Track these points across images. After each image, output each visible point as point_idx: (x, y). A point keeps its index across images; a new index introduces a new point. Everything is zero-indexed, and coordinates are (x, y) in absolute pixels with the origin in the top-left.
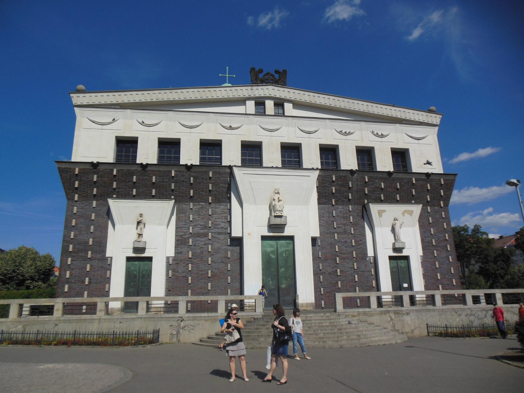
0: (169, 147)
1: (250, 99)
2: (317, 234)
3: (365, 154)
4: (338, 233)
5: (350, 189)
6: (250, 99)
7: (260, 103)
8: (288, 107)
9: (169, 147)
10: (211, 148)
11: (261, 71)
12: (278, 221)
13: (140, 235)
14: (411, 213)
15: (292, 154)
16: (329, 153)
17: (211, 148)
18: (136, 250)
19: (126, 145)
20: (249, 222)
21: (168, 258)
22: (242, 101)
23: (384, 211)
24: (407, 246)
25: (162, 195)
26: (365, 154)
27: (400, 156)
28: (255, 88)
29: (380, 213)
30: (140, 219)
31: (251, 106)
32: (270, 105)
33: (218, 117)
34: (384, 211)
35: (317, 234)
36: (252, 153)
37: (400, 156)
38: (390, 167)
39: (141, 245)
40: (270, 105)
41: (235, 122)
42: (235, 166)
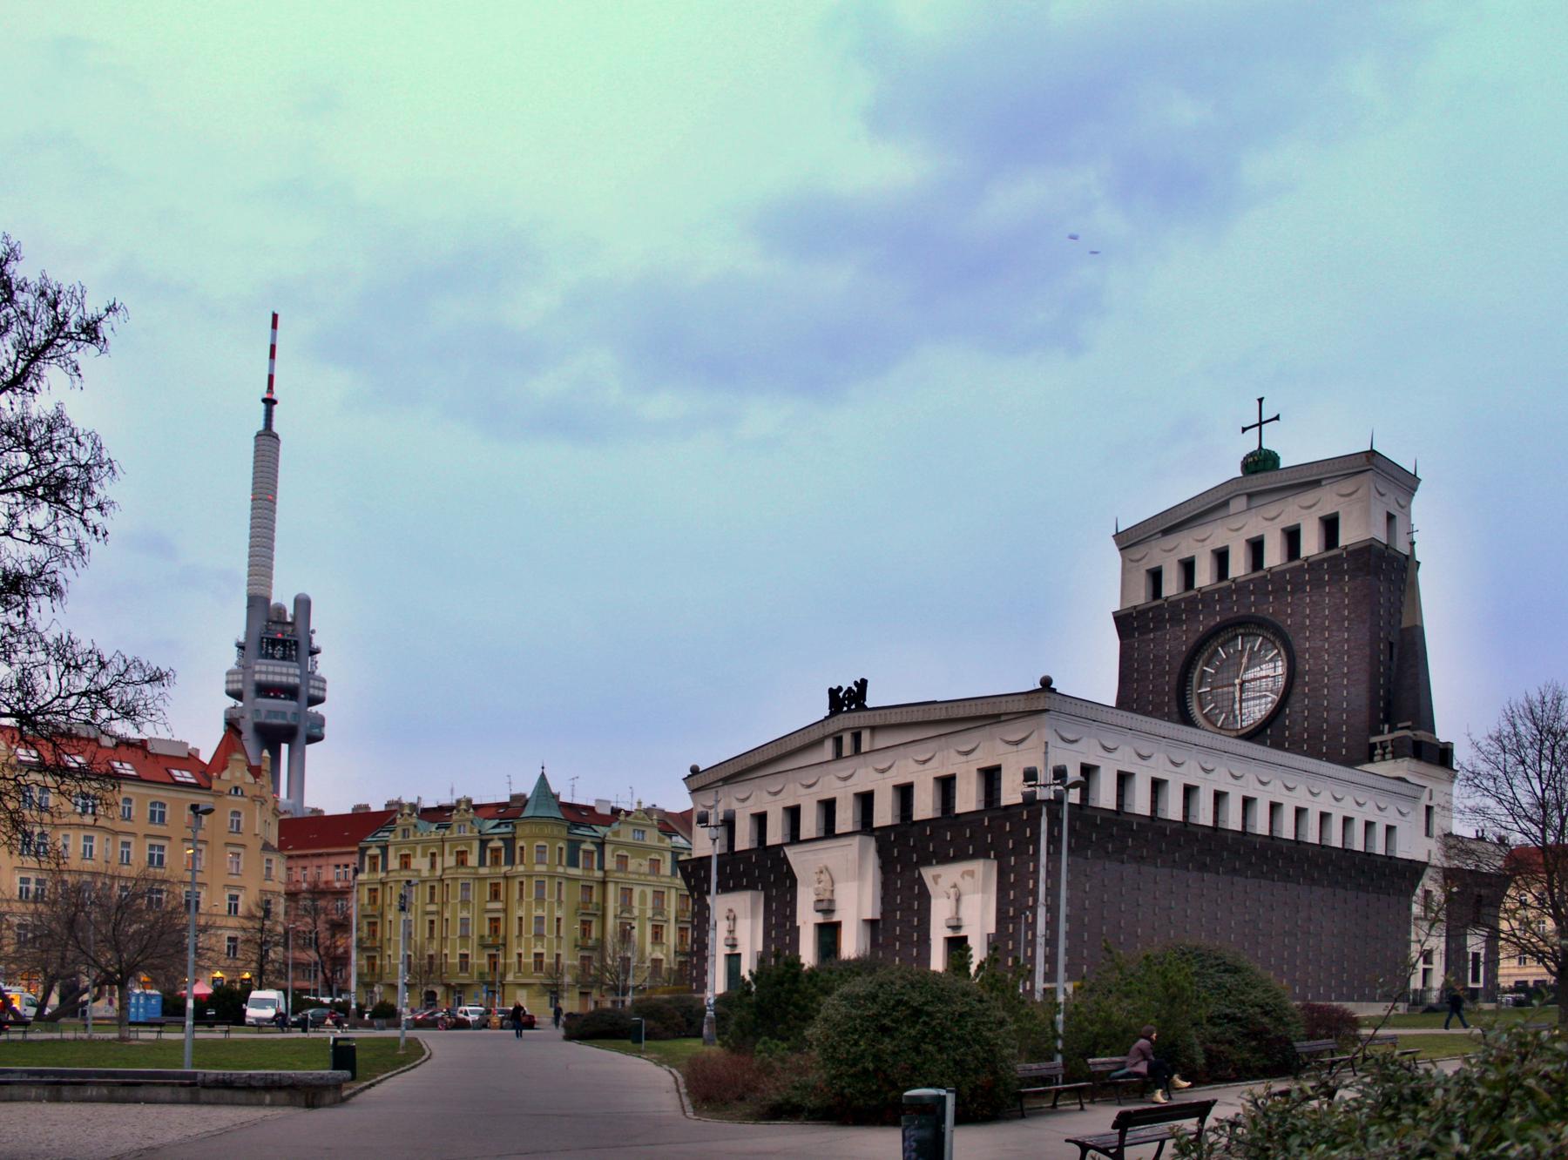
1: (826, 737)
4: (902, 911)
5: (907, 849)
6: (826, 737)
7: (838, 741)
8: (866, 736)
11: (840, 689)
14: (971, 874)
22: (819, 743)
24: (965, 922)
29: (936, 878)
31: (828, 750)
32: (847, 739)
33: (798, 774)
40: (847, 739)
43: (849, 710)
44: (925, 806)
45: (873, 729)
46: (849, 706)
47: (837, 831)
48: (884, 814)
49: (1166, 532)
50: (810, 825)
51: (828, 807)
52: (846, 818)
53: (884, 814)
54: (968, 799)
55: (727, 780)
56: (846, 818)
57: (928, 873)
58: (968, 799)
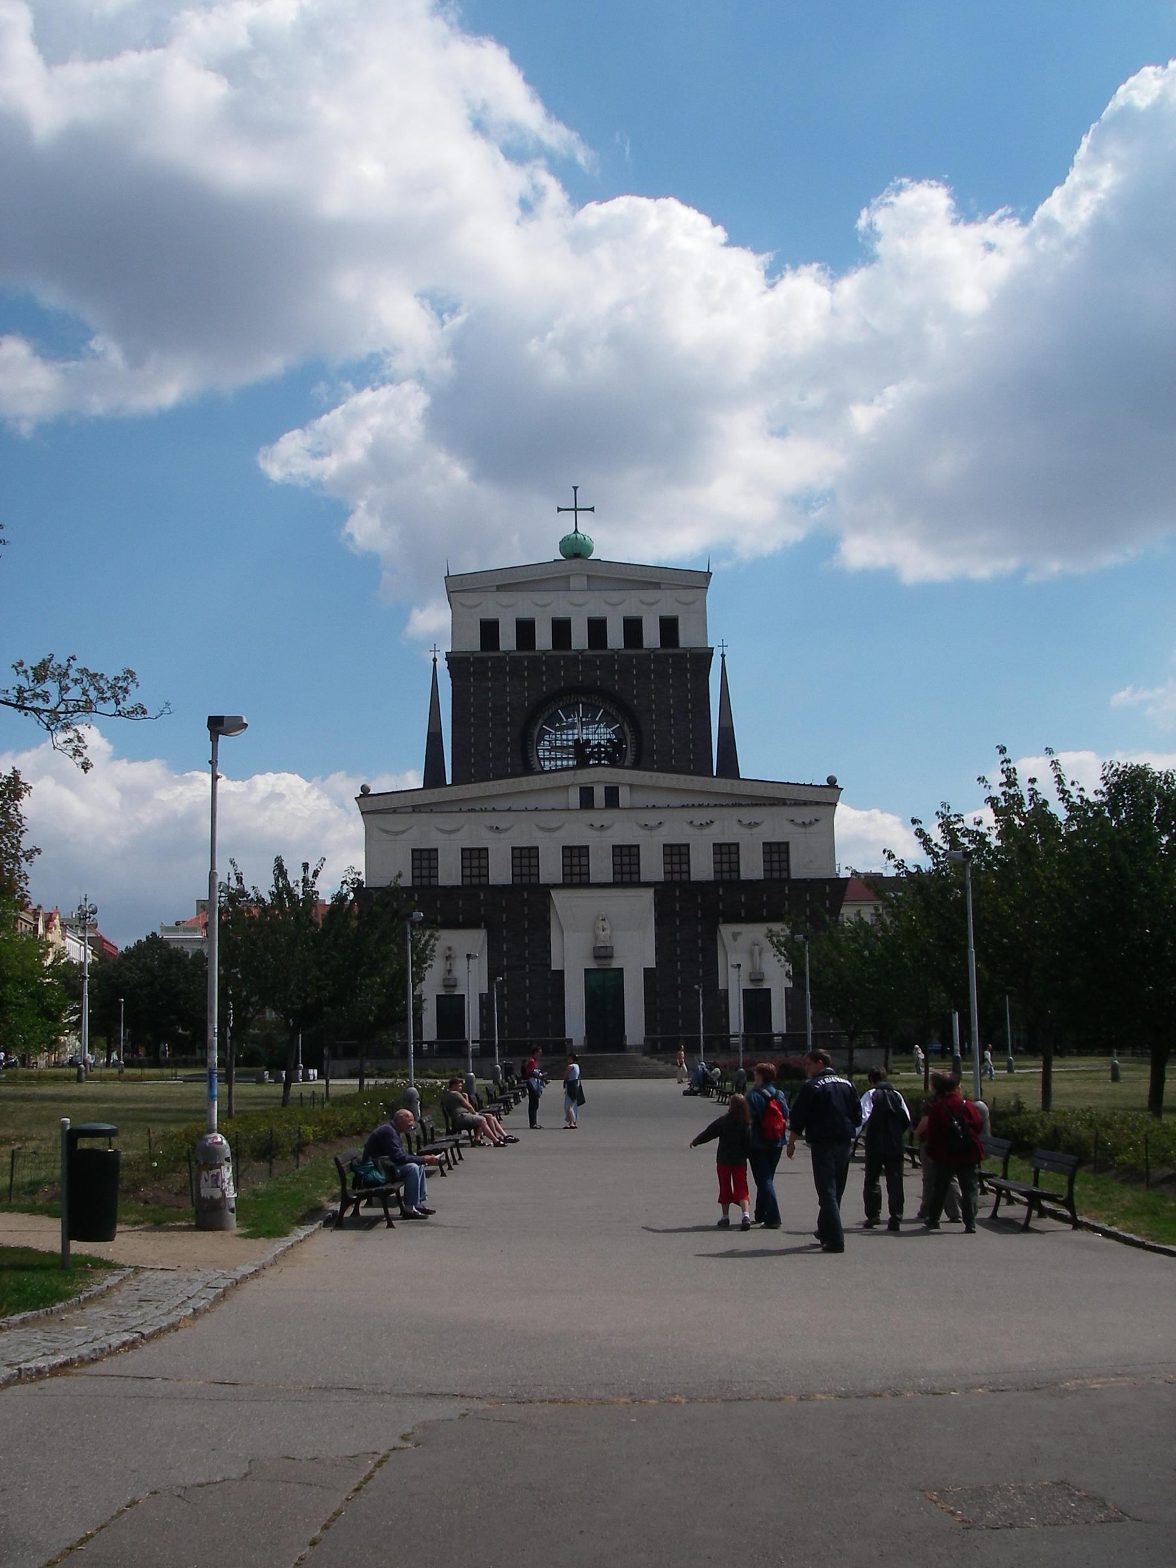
0: (475, 857)
2: (652, 964)
3: (726, 853)
9: (475, 857)
10: (525, 857)
12: (603, 952)
13: (450, 971)
15: (626, 858)
16: (677, 853)
17: (525, 857)
18: (446, 986)
19: (424, 859)
20: (570, 955)
21: (481, 995)
23: (740, 934)
25: (470, 924)
26: (726, 853)
27: (777, 852)
28: (579, 772)
29: (735, 936)
30: (448, 953)
31: (574, 798)
32: (599, 794)
34: (740, 934)
35: (652, 964)
36: (575, 858)
37: (777, 852)
38: (759, 874)
39: (451, 983)
40: (599, 794)
41: (553, 820)
42: (556, 886)
43: (600, 765)
44: (702, 867)
45: (631, 786)
46: (600, 759)
47: (592, 880)
48: (652, 867)
49: (499, 588)
50: (550, 869)
51: (575, 856)
52: (601, 867)
53: (652, 867)
54: (752, 867)
55: (416, 809)
56: (601, 867)
57: (726, 931)
58: (752, 867)
